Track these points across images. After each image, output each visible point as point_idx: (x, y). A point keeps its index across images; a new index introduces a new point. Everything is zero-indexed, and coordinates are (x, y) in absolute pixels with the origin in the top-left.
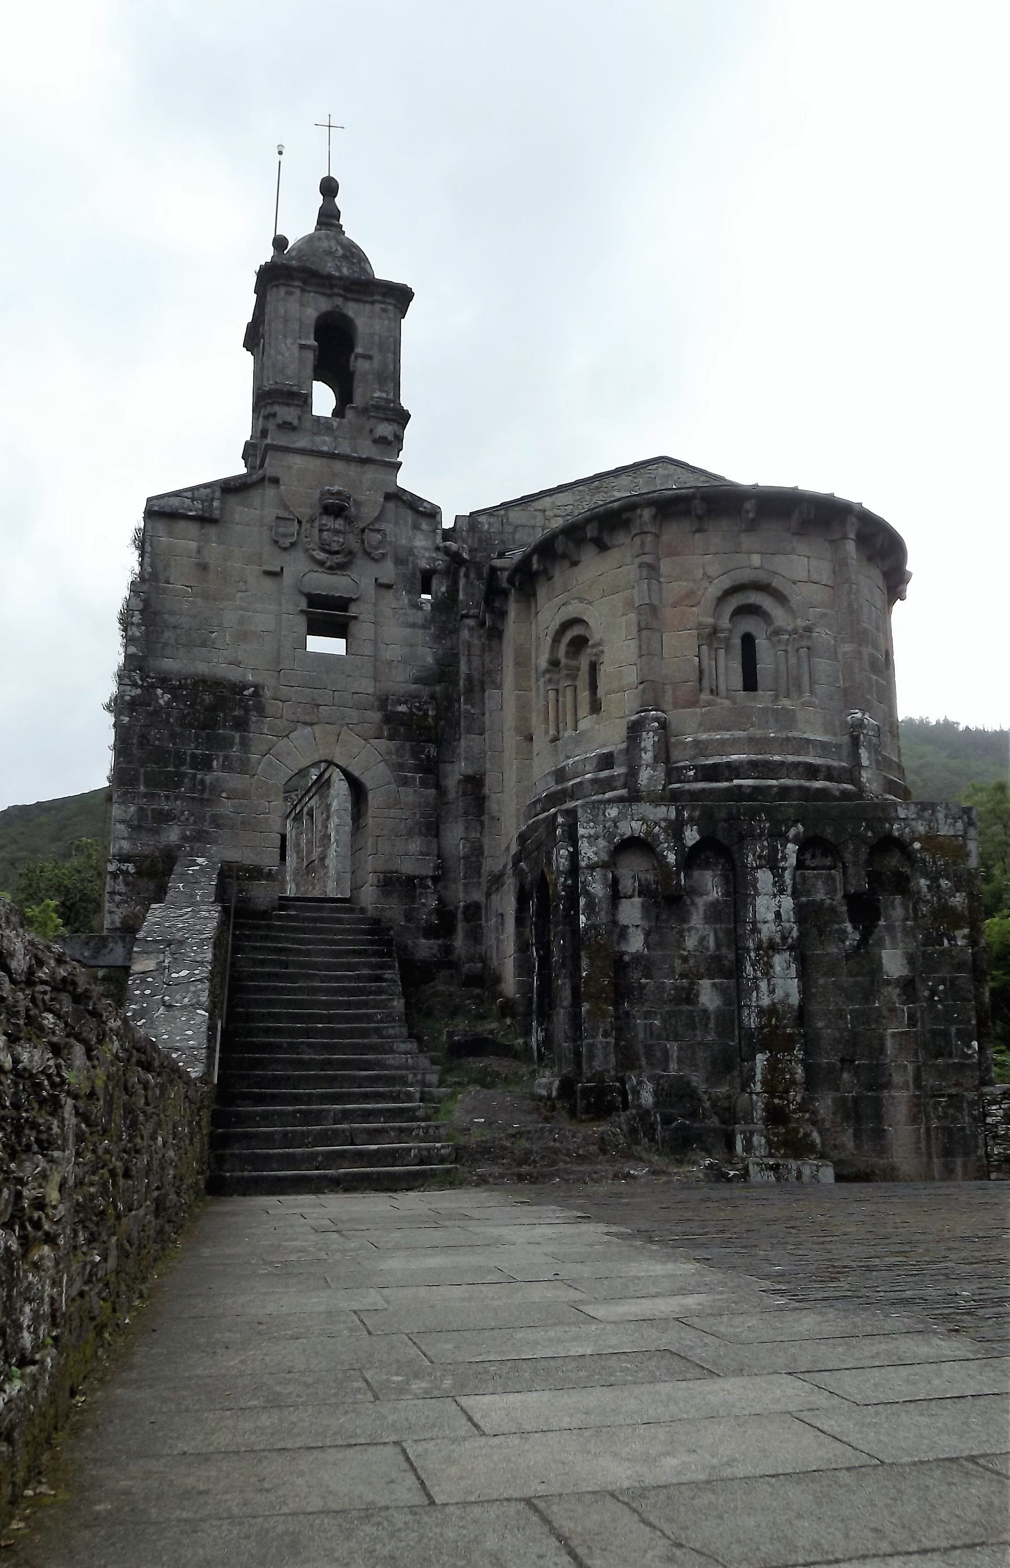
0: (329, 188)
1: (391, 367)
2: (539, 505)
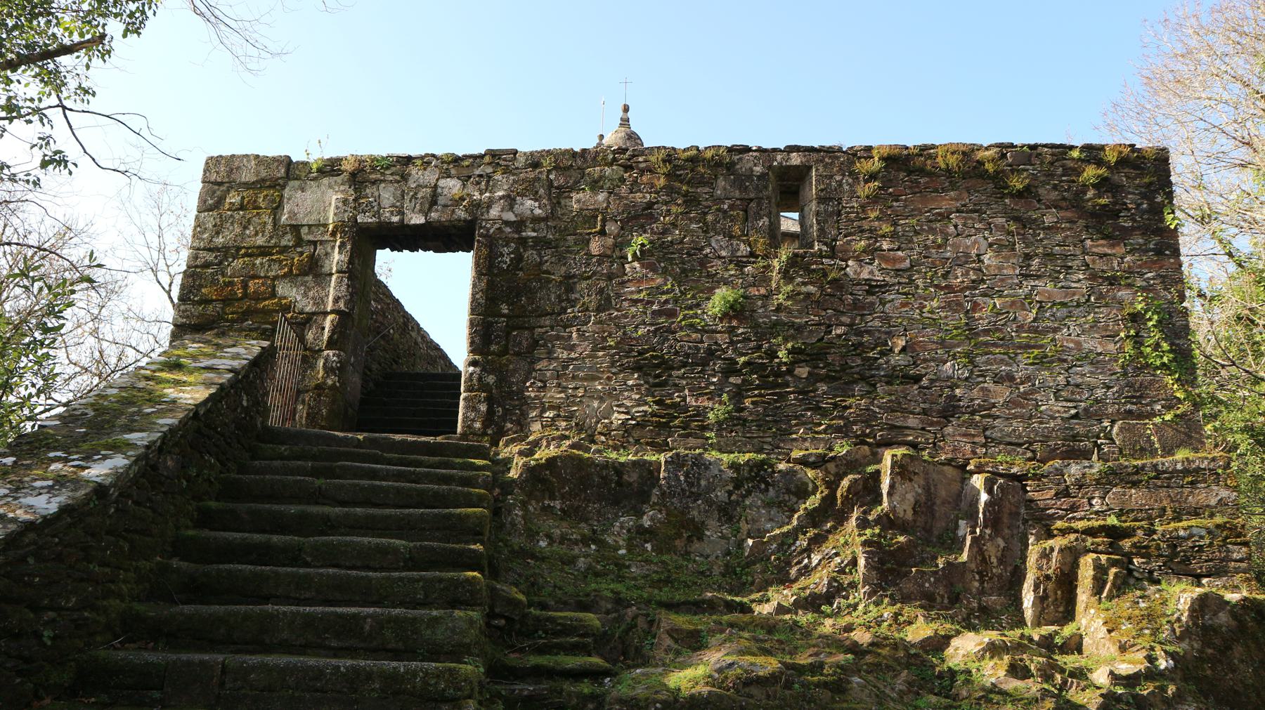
0: (626, 109)
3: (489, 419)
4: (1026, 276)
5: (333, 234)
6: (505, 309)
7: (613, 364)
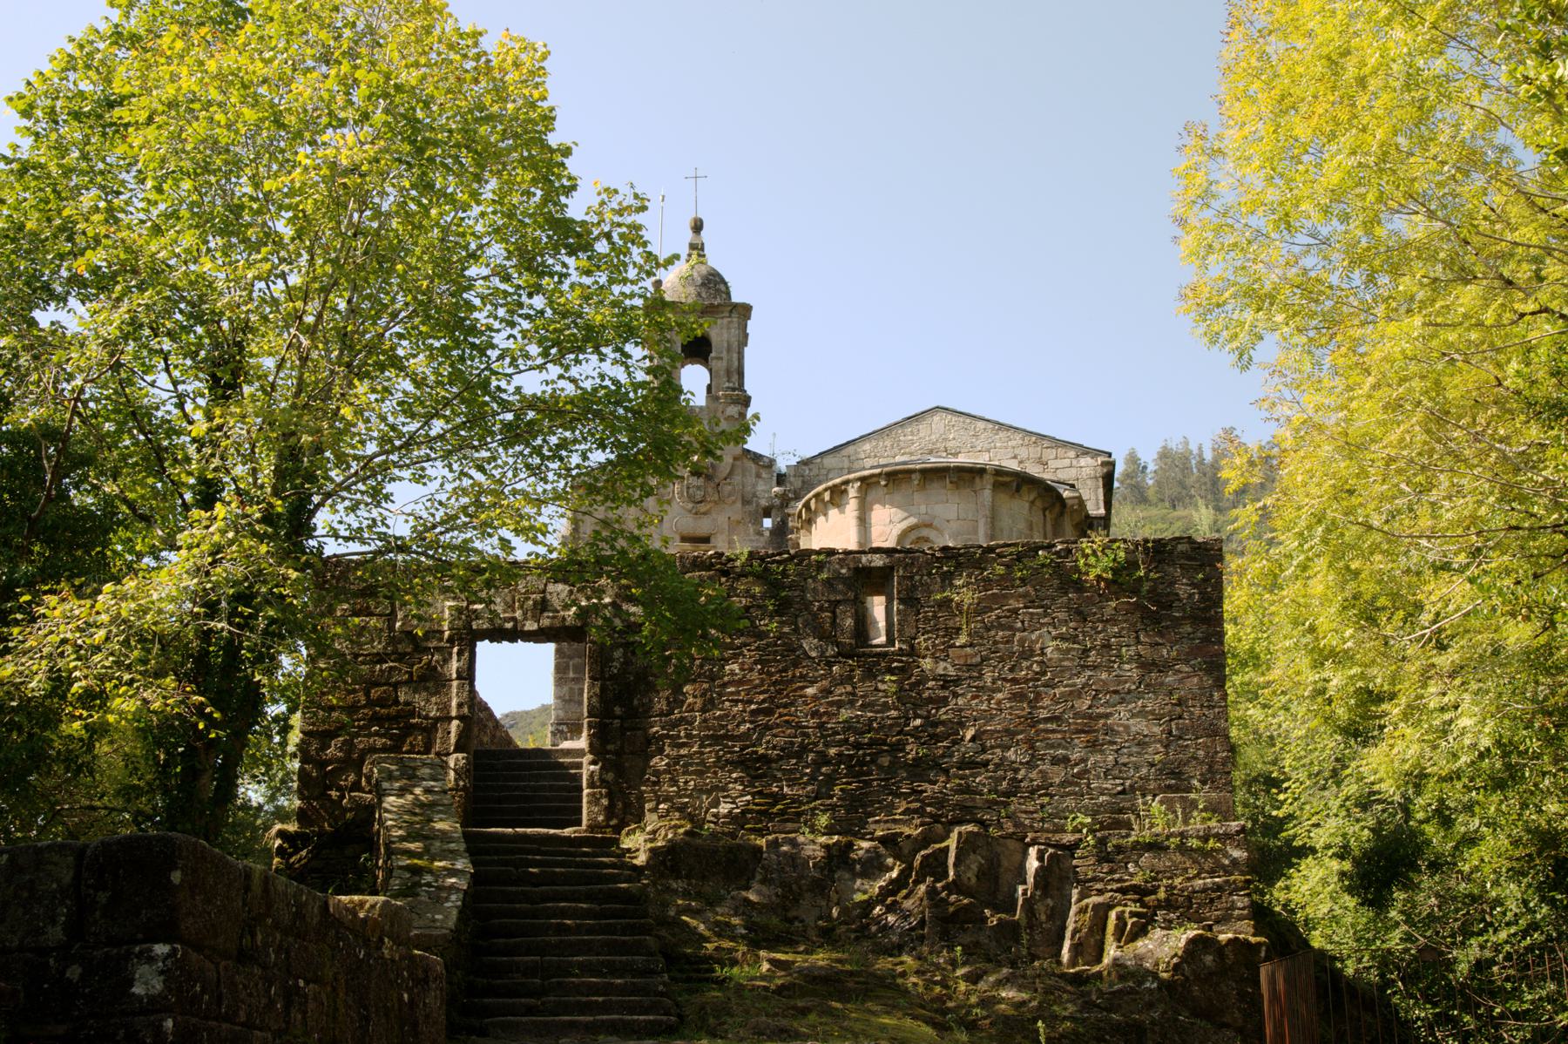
0: (698, 227)
1: (736, 364)
2: (845, 452)
3: (609, 811)
4: (1084, 667)
5: (451, 640)
6: (618, 710)
7: (719, 758)
